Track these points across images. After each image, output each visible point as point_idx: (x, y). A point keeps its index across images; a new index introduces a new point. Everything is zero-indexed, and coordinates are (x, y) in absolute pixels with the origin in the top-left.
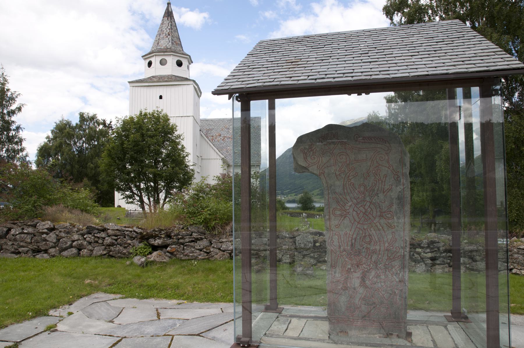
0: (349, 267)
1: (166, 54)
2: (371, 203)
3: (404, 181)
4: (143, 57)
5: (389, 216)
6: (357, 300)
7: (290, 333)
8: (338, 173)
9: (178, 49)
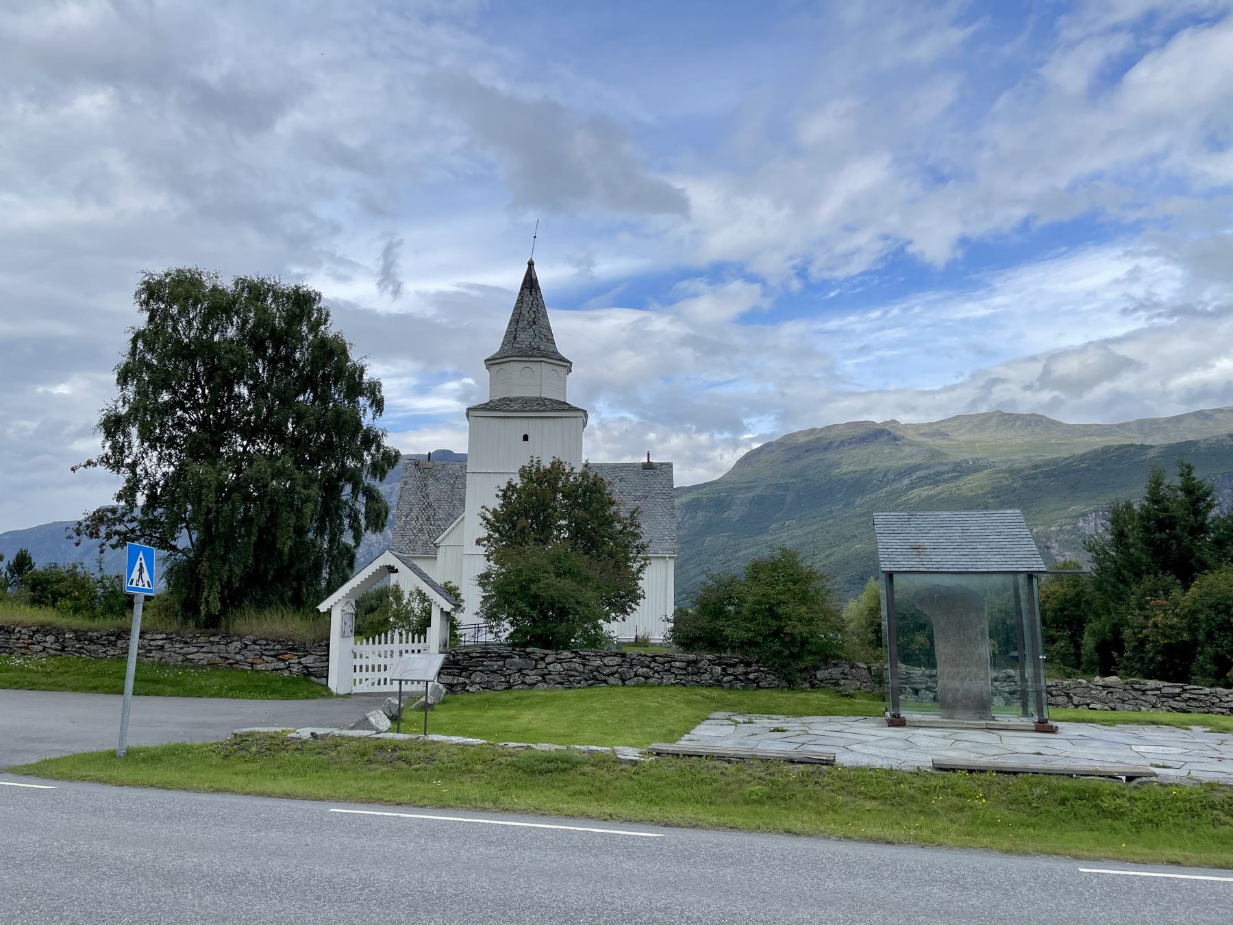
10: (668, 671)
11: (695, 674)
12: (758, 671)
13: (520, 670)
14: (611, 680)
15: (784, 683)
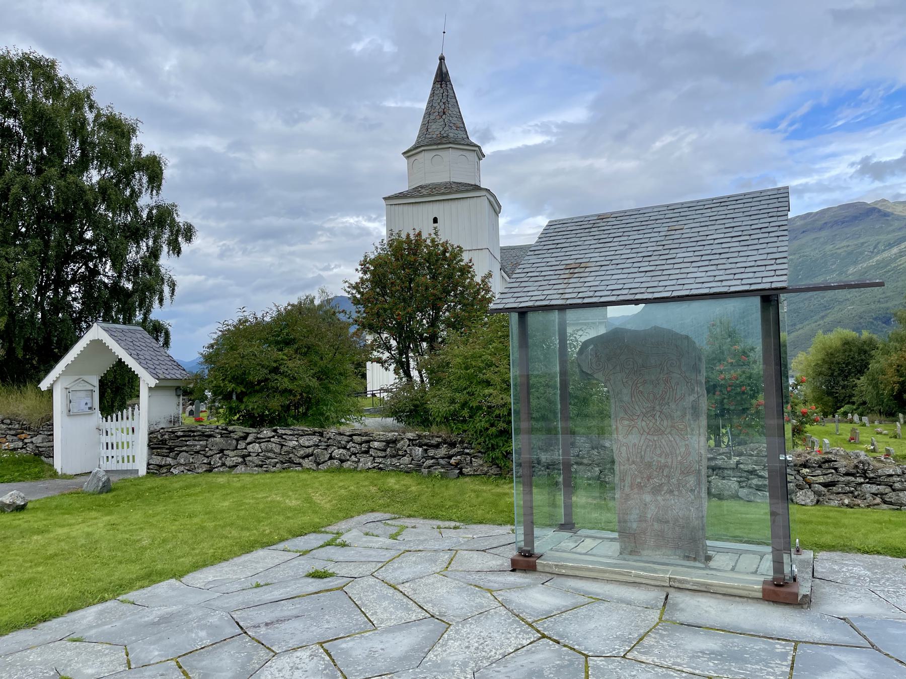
1: (440, 147)
4: (404, 154)
7: (579, 549)
8: (625, 380)
9: (460, 136)
10: (367, 452)
11: (394, 456)
12: (461, 453)
13: (222, 451)
14: (307, 463)
15: (494, 470)
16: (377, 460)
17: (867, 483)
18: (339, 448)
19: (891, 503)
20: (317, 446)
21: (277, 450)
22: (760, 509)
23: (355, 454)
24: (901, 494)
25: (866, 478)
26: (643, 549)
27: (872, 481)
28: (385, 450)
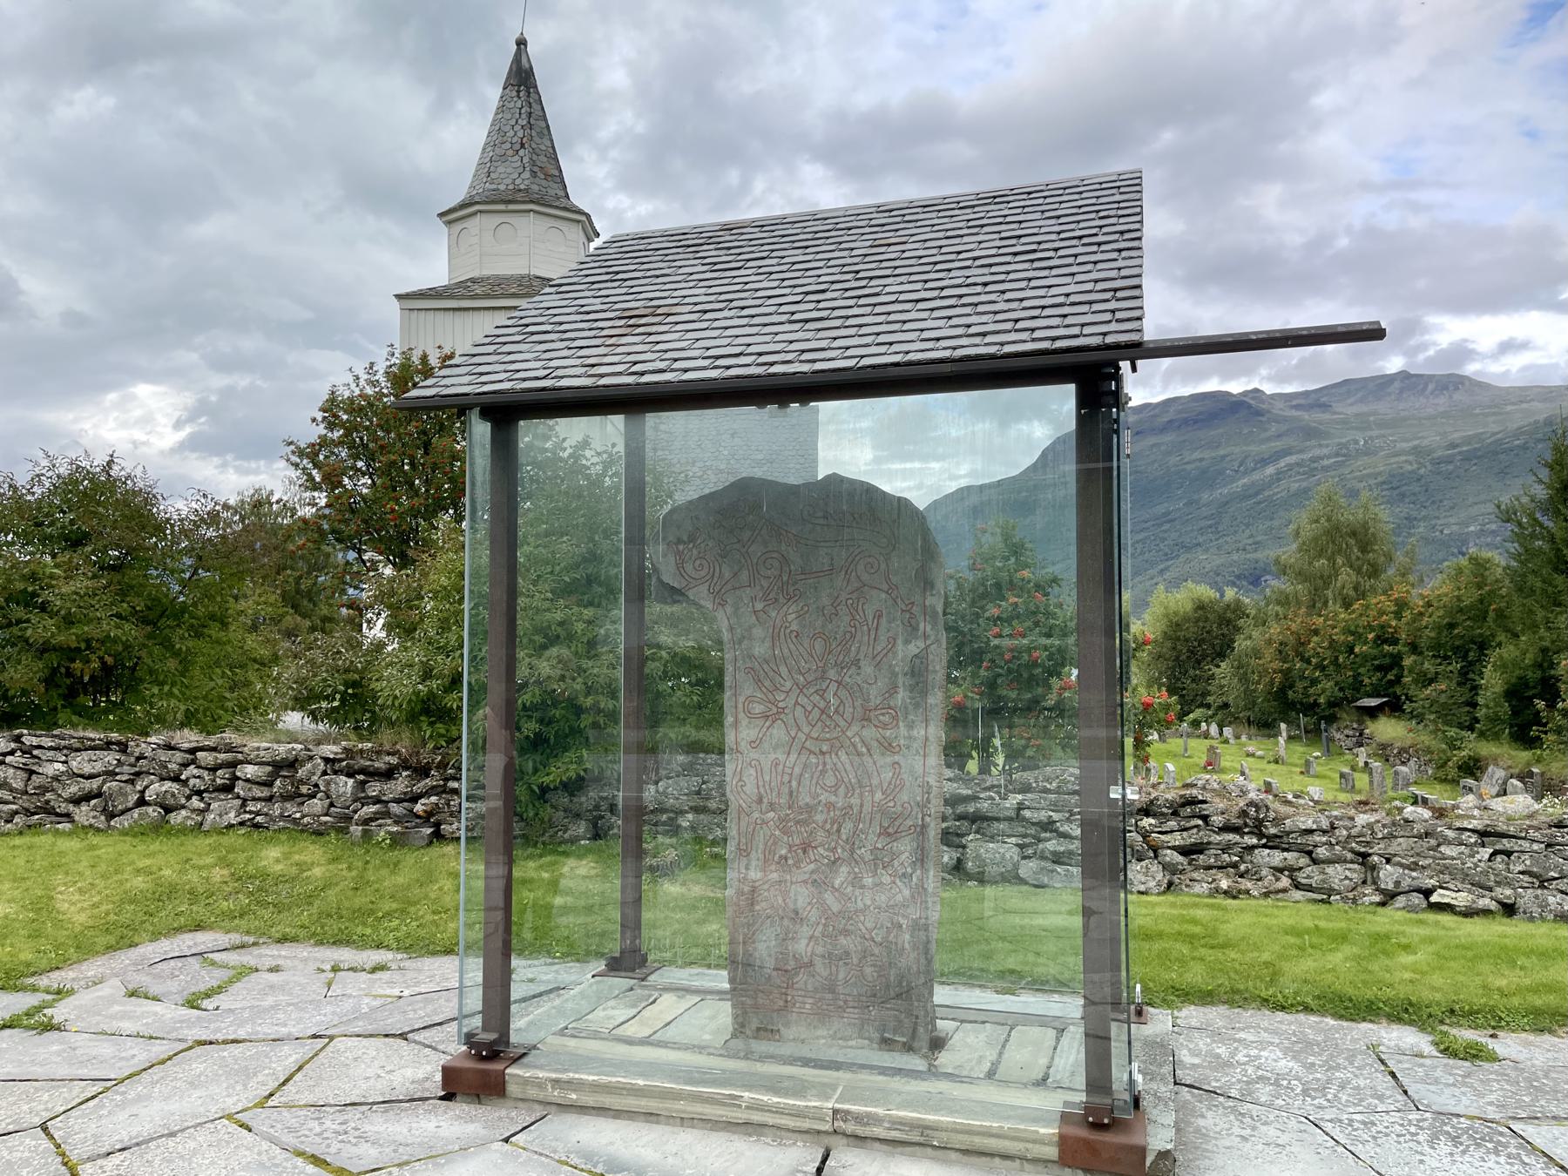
0: (783, 852)
1: (511, 207)
2: (840, 683)
3: (928, 628)
4: (441, 215)
5: (886, 719)
6: (804, 942)
9: (552, 192)
10: (228, 789)
11: (287, 798)
14: (83, 814)
16: (251, 807)
17: (1264, 846)
18: (163, 779)
19: (1309, 888)
20: (111, 774)
21: (18, 784)
22: (1057, 908)
23: (199, 793)
24: (1330, 870)
25: (1261, 835)
26: (787, 1025)
27: (1273, 843)
28: (269, 784)
